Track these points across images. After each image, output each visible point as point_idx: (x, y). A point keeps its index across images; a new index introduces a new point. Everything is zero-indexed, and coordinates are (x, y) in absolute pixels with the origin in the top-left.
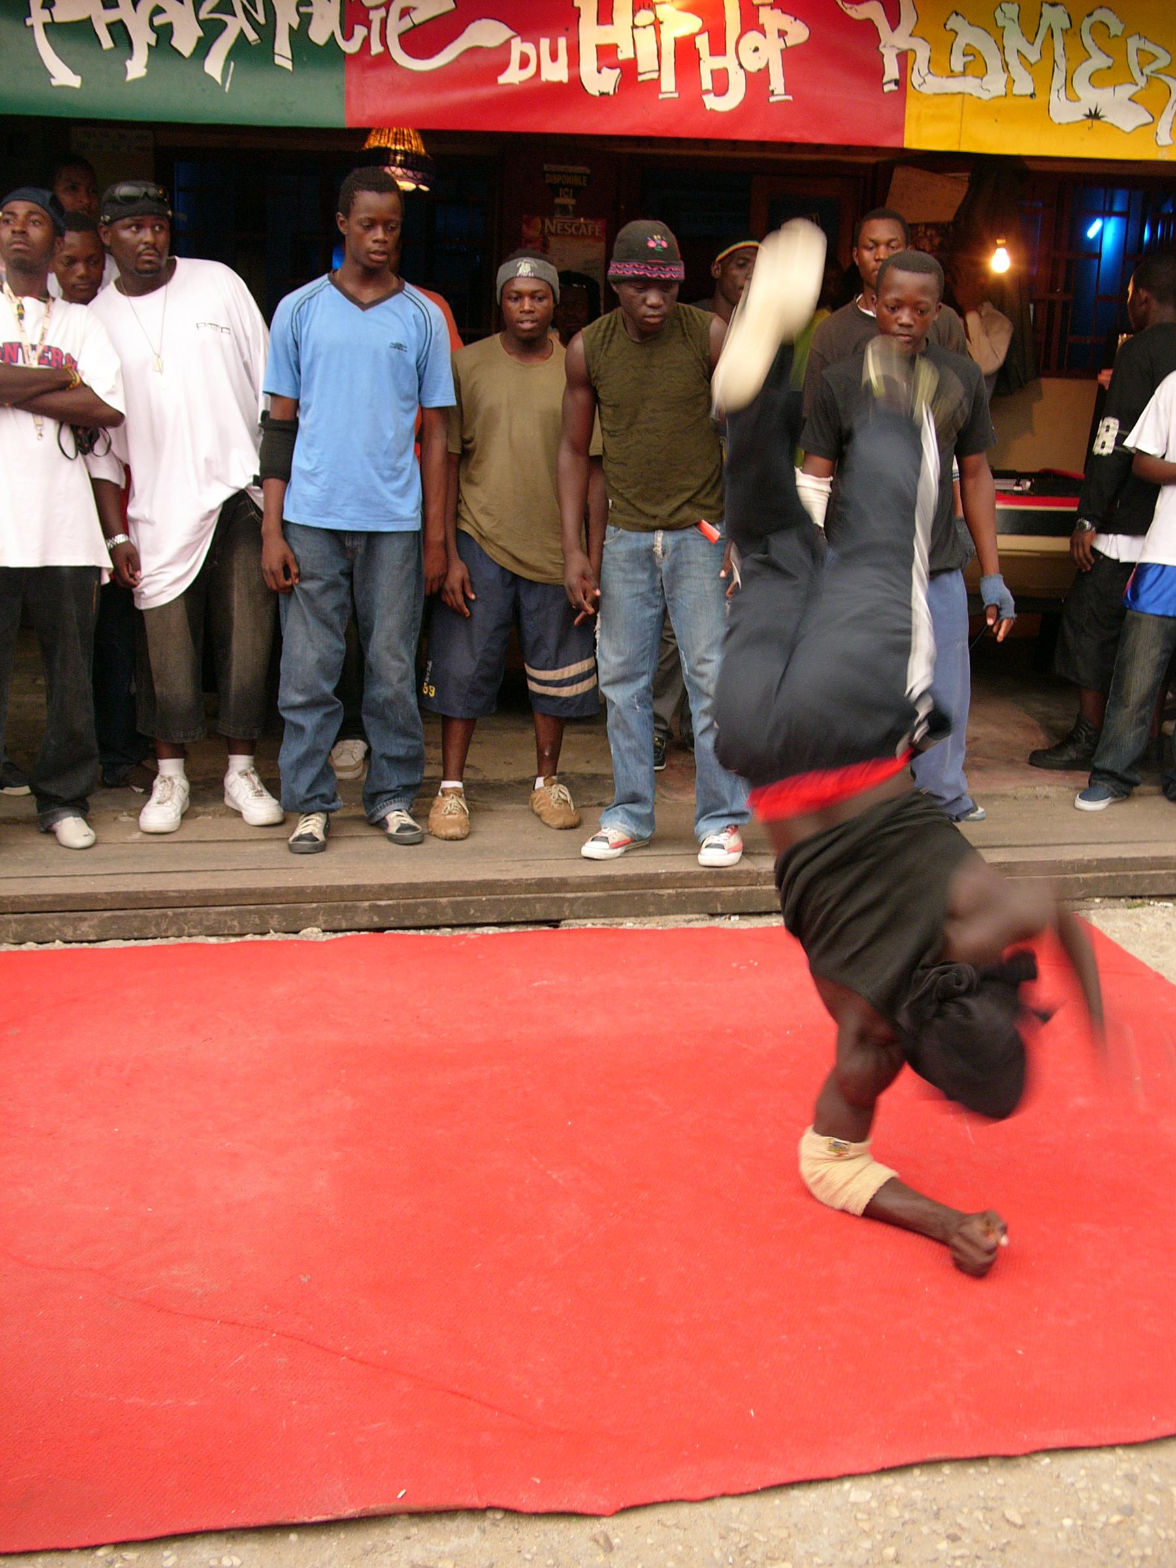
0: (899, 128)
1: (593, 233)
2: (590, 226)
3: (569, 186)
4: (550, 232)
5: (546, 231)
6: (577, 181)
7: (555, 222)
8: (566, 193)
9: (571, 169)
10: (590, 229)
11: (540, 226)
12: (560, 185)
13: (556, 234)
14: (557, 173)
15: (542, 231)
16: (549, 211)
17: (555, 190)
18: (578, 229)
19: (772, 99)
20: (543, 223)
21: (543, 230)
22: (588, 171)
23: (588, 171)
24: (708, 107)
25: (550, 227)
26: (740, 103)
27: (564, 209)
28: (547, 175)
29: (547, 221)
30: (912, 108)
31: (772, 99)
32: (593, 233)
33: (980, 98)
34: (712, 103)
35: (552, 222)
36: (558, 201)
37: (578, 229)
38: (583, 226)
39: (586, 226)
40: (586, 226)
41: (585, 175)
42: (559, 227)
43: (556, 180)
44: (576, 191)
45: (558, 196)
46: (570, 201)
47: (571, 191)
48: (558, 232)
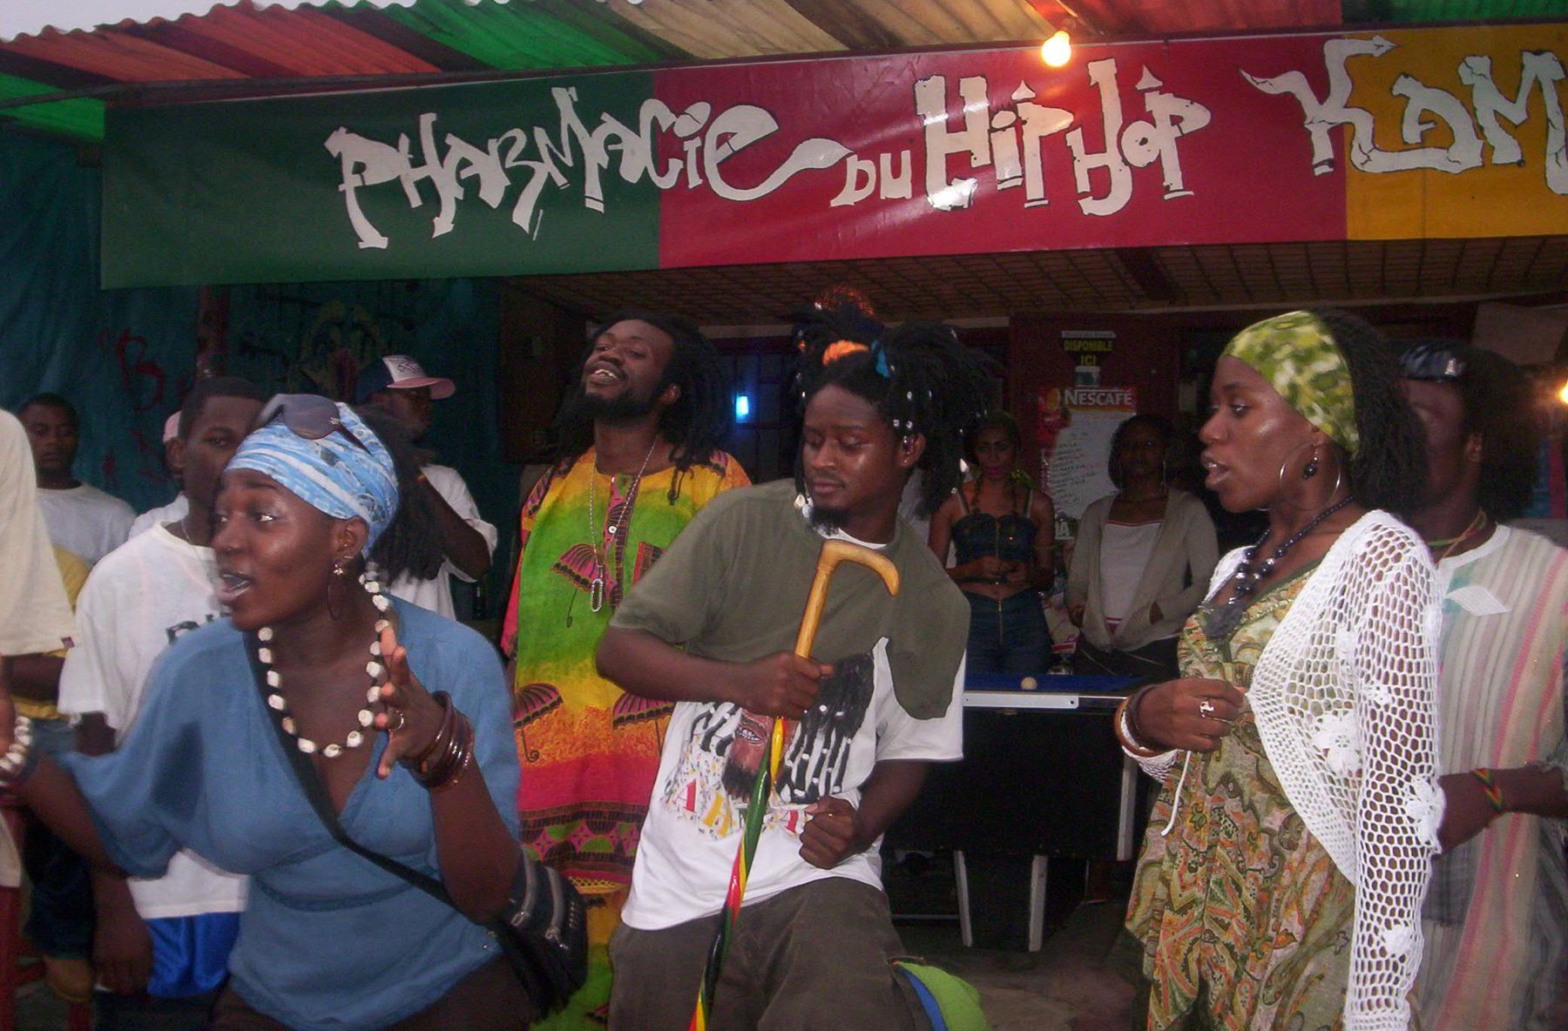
0: (1340, 219)
1: (1122, 402)
2: (1117, 395)
3: (1092, 353)
4: (1071, 405)
5: (1066, 402)
6: (1101, 347)
7: (1076, 391)
8: (1089, 360)
9: (1092, 334)
10: (1118, 399)
11: (1059, 398)
12: (1082, 352)
13: (1078, 407)
14: (1078, 339)
15: (1062, 404)
16: (1069, 380)
17: (1076, 357)
18: (1103, 398)
19: (1167, 197)
20: (1063, 395)
21: (1062, 404)
22: (1114, 336)
23: (1114, 336)
24: (1086, 213)
25: (1071, 398)
26: (1127, 204)
27: (1087, 378)
28: (1066, 342)
29: (1067, 392)
30: (1353, 193)
31: (1167, 197)
32: (1122, 402)
33: (1435, 169)
34: (1089, 206)
35: (1073, 394)
36: (1079, 369)
37: (1103, 398)
38: (1110, 395)
39: (1113, 394)
40: (1113, 394)
41: (1110, 339)
42: (1081, 395)
43: (1077, 347)
44: (1101, 358)
45: (1079, 364)
46: (1094, 370)
47: (1095, 357)
48: (1081, 403)
